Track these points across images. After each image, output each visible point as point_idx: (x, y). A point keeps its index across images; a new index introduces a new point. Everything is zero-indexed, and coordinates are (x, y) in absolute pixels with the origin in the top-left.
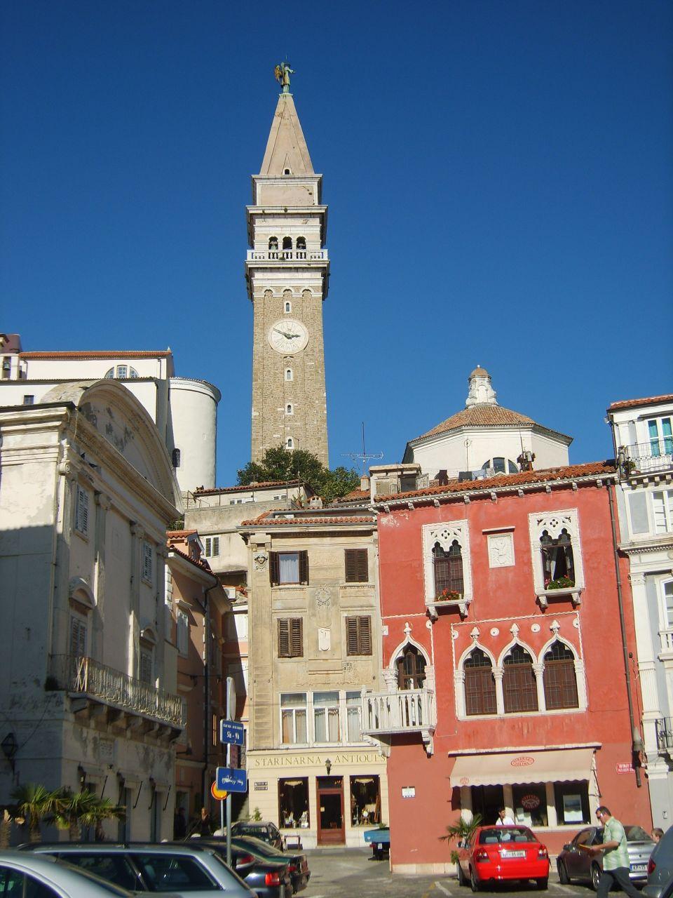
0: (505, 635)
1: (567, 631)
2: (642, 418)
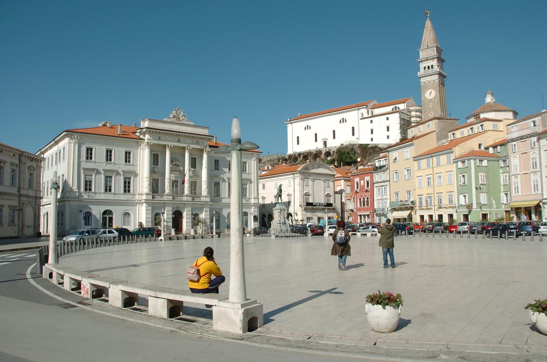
0: (362, 195)
1: (368, 195)
2: (378, 161)
